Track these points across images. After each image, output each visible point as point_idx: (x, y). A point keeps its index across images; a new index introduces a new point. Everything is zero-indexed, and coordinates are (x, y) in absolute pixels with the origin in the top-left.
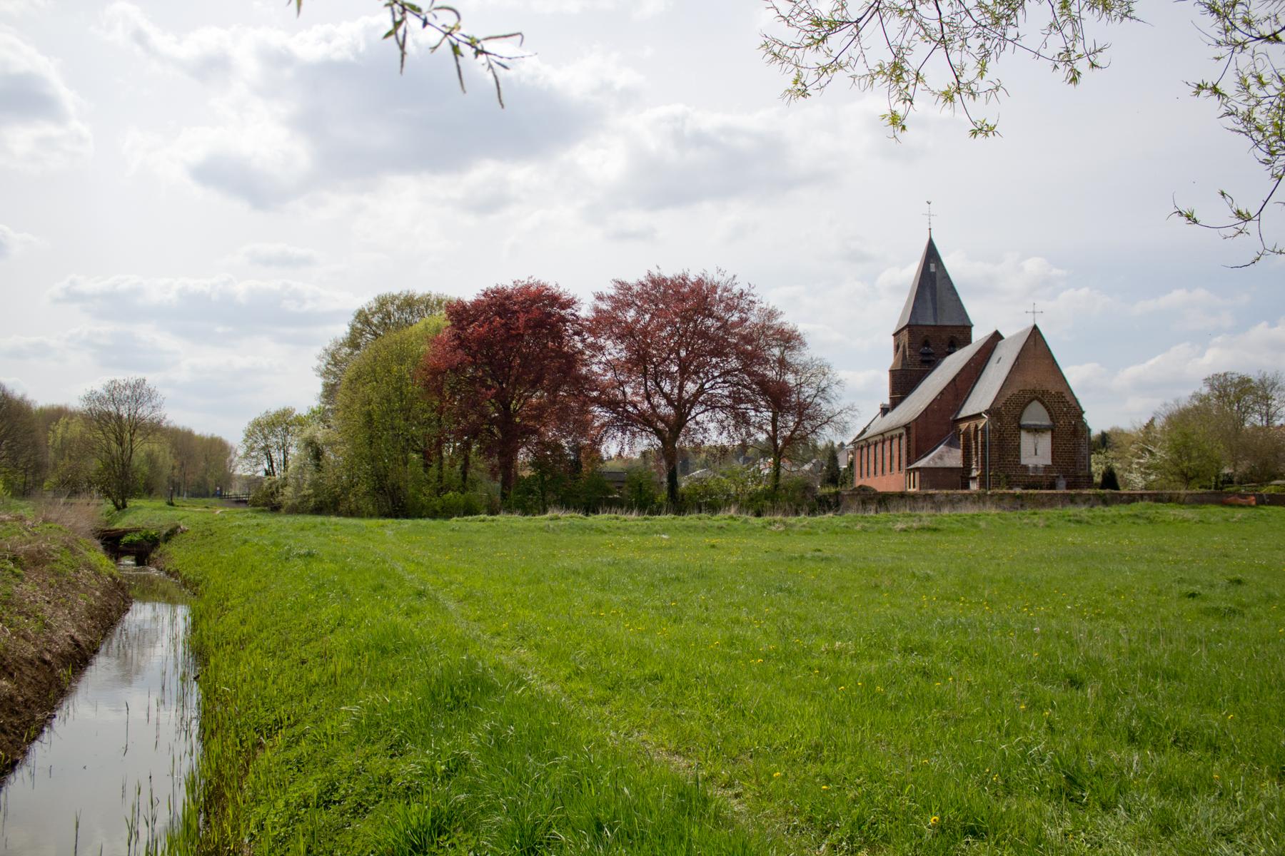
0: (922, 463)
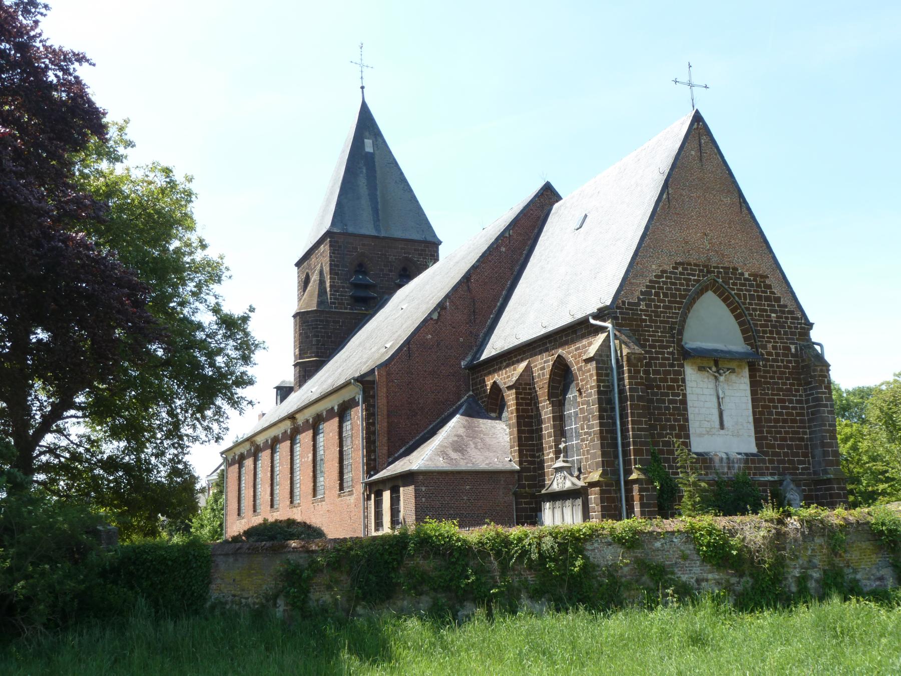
0: (420, 460)
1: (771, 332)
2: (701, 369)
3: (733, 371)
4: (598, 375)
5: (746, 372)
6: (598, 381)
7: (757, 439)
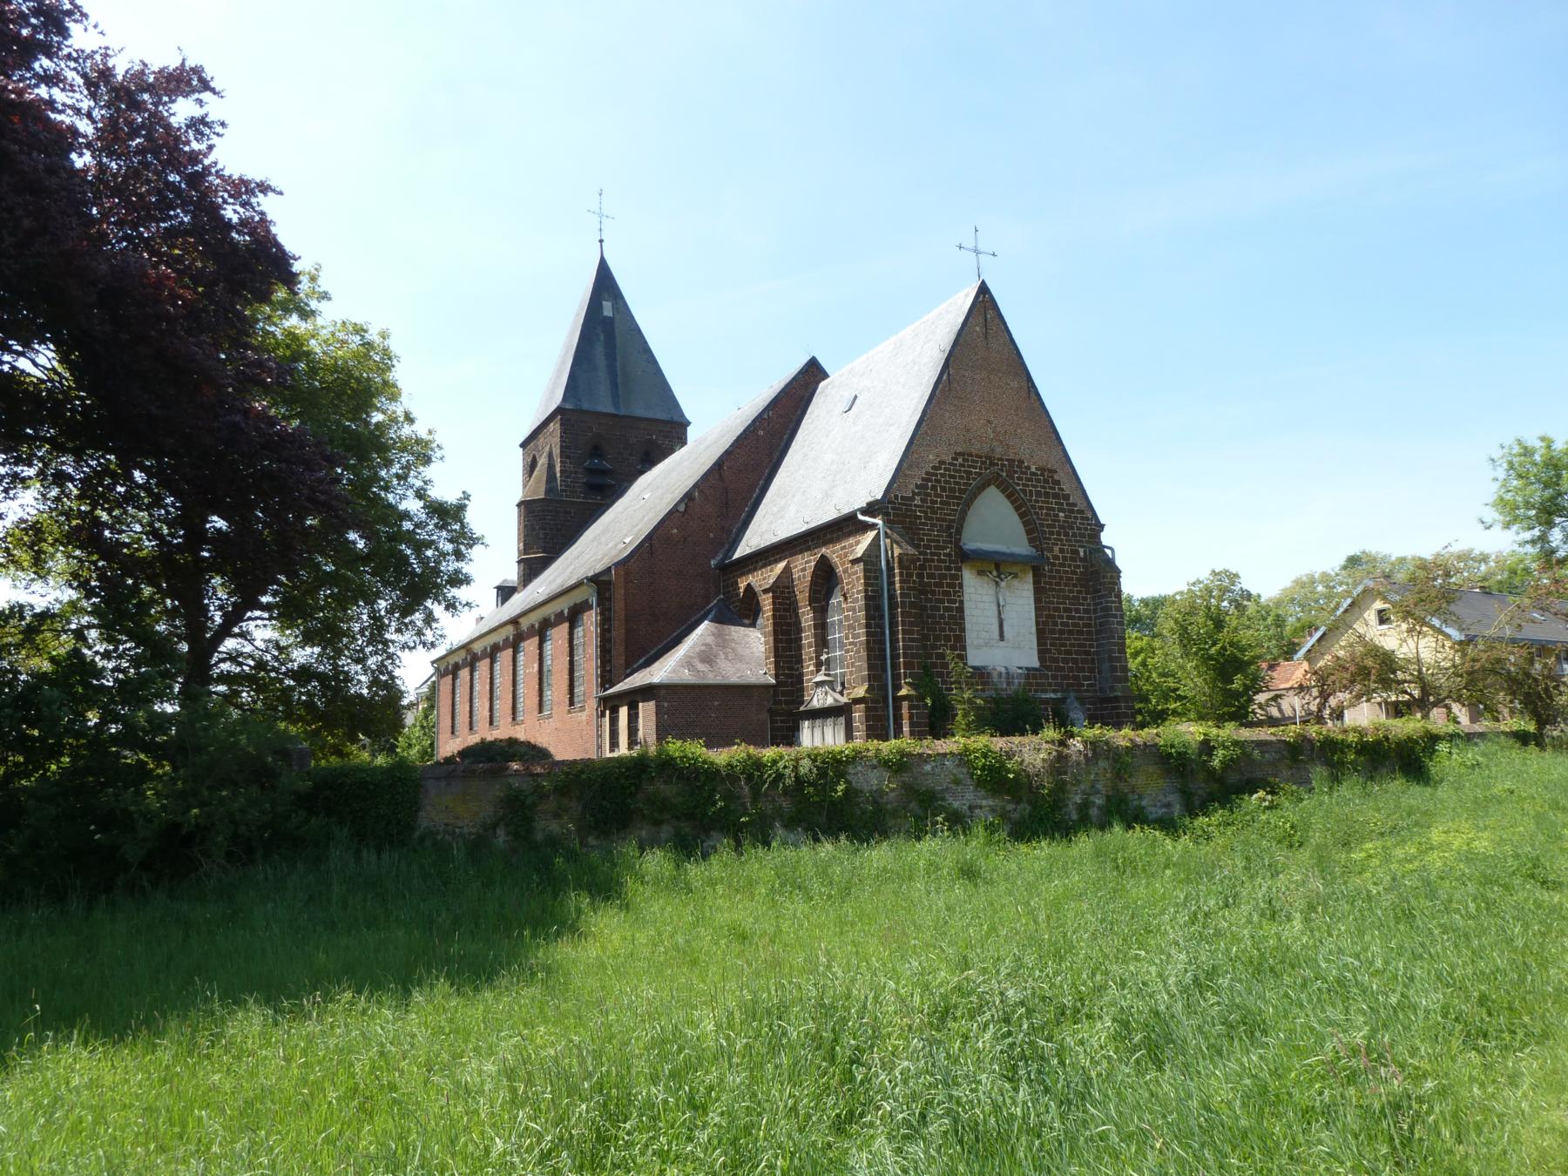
0: (662, 672)
1: (1059, 534)
2: (981, 573)
3: (1016, 576)
4: (866, 578)
5: (1030, 578)
6: (866, 584)
7: (1040, 652)
